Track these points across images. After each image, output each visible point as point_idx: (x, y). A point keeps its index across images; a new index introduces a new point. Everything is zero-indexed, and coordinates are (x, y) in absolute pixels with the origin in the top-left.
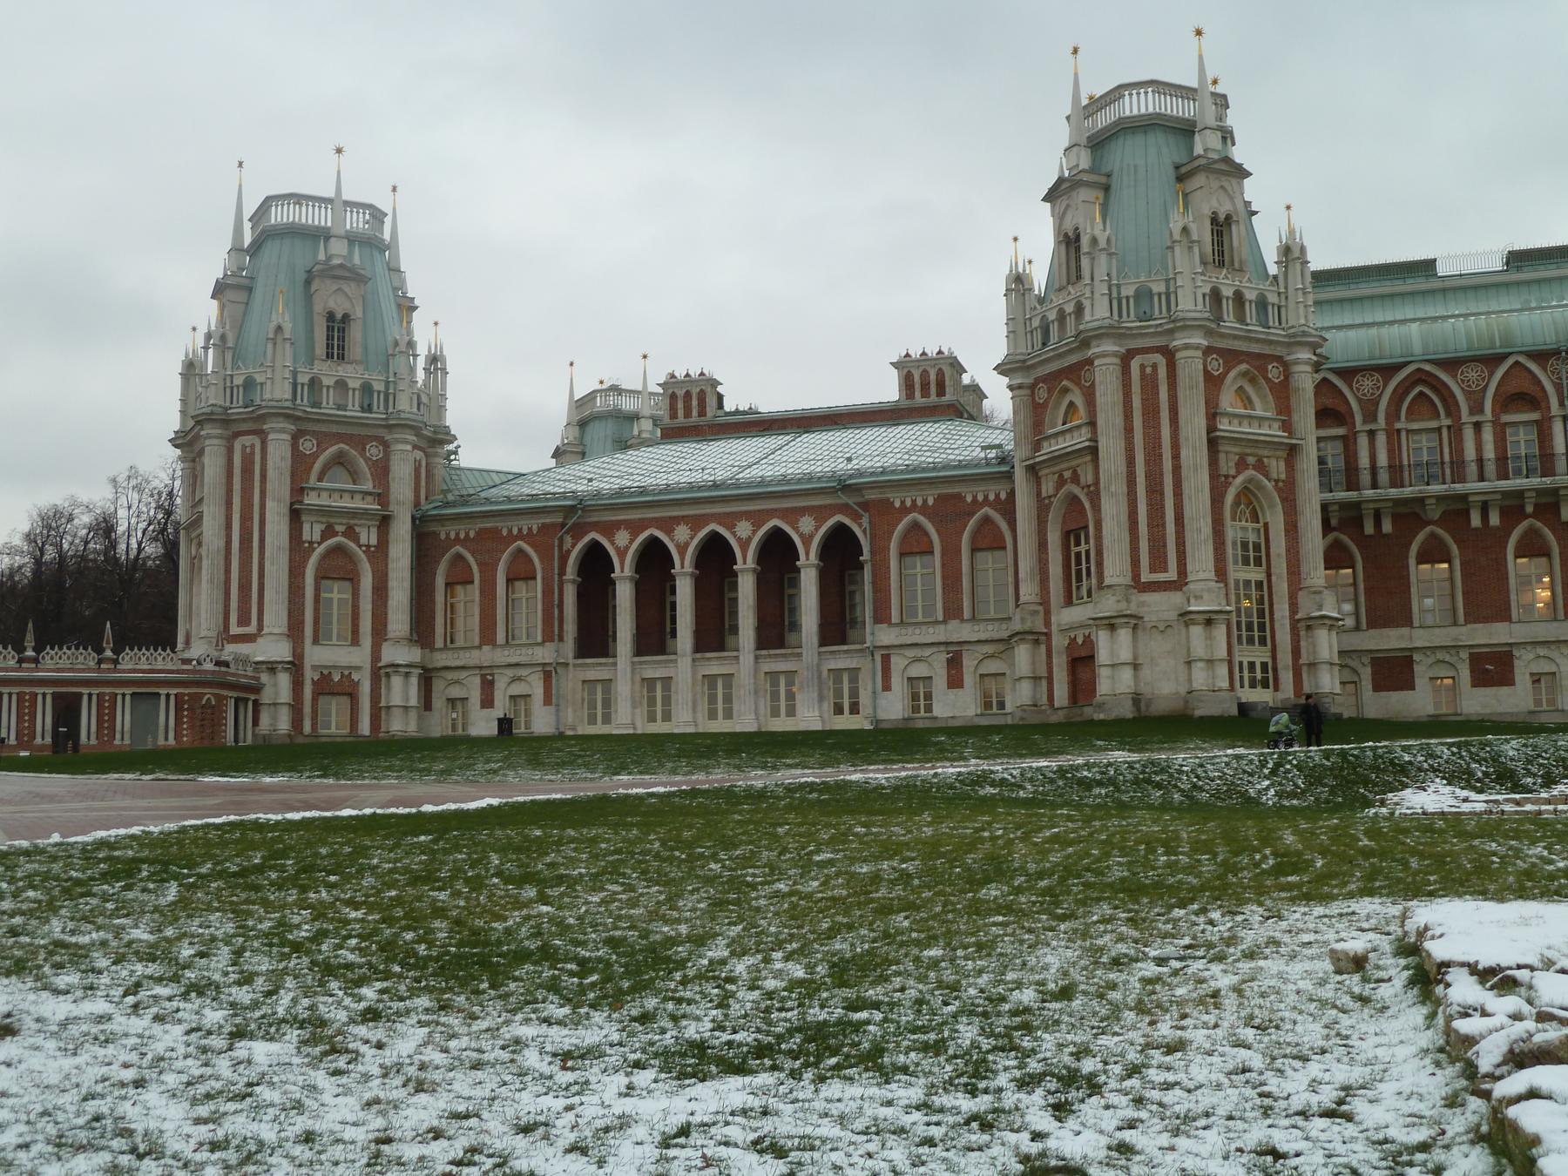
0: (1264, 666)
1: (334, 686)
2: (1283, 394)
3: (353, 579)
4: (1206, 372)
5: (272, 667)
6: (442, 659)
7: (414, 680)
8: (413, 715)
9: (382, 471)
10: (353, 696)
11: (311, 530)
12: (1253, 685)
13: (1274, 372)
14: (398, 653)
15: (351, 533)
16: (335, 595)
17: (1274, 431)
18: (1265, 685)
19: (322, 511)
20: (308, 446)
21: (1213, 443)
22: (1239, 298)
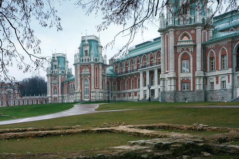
0: (88, 97)
1: (55, 98)
2: (90, 69)
3: (56, 89)
4: (80, 67)
5: (49, 97)
6: (64, 95)
7: (61, 97)
8: (61, 101)
9: (58, 79)
10: (57, 99)
11: (53, 85)
12: (87, 98)
13: (89, 66)
14: (60, 95)
15: (56, 85)
16: (56, 90)
17: (89, 73)
18: (88, 98)
19: (53, 83)
20: (52, 77)
21: (81, 75)
22: (85, 59)
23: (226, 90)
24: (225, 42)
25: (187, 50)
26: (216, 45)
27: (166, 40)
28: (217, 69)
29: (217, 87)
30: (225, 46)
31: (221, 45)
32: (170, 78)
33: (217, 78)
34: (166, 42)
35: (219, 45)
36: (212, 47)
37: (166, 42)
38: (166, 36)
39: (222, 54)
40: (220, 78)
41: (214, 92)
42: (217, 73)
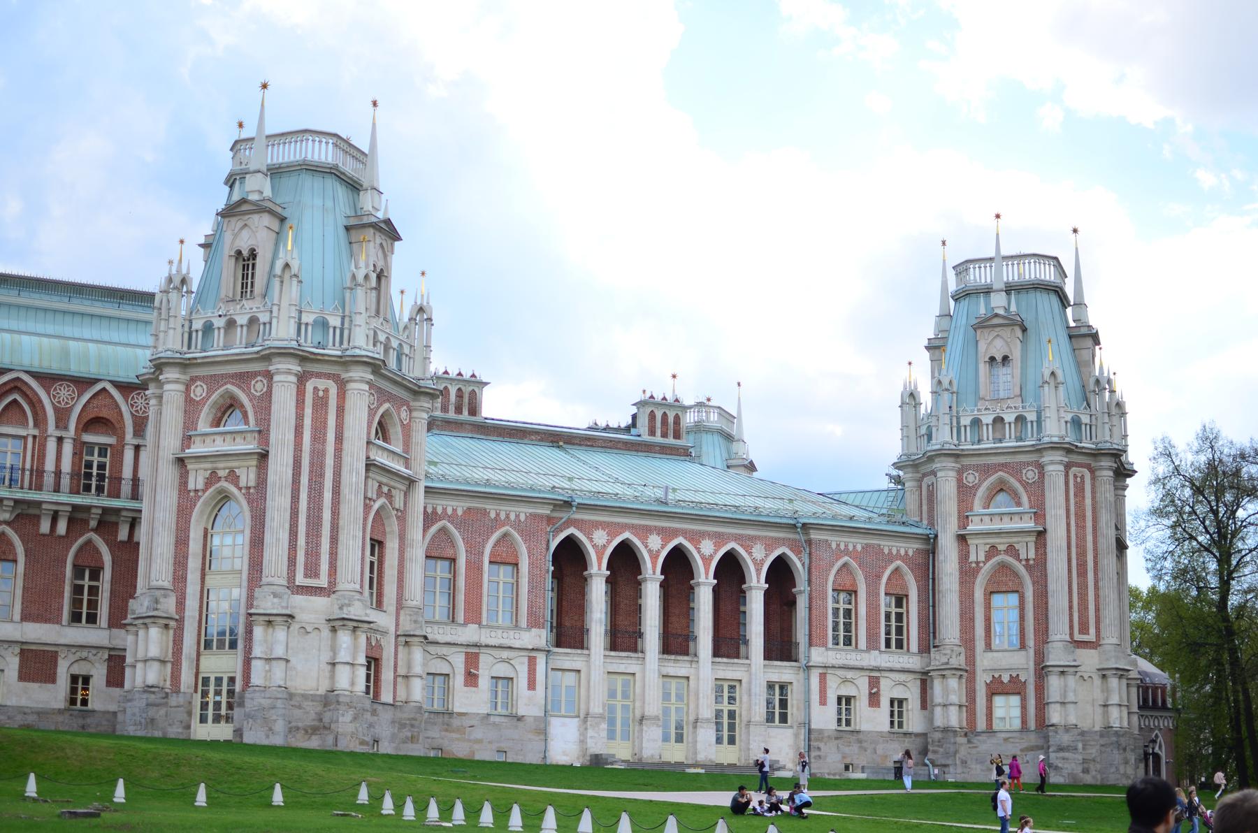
23: (520, 719)
24: (524, 511)
25: (389, 496)
26: (469, 509)
27: (308, 411)
28: (474, 616)
29: (470, 701)
30: (517, 525)
31: (498, 515)
32: (356, 625)
33: (472, 661)
34: (308, 422)
35: (485, 513)
36: (450, 511)
37: (308, 422)
38: (310, 386)
39: (492, 554)
40: (485, 659)
41: (456, 722)
42: (469, 634)
